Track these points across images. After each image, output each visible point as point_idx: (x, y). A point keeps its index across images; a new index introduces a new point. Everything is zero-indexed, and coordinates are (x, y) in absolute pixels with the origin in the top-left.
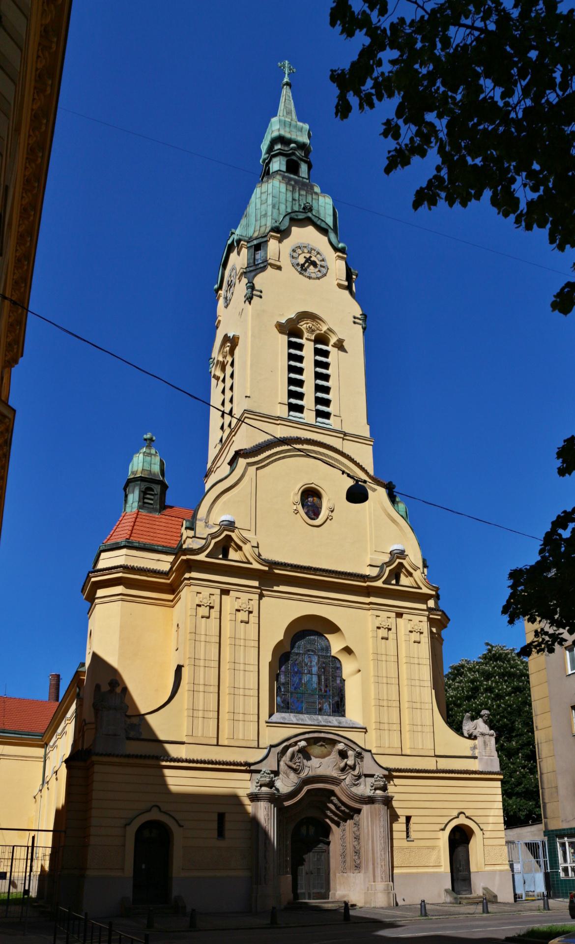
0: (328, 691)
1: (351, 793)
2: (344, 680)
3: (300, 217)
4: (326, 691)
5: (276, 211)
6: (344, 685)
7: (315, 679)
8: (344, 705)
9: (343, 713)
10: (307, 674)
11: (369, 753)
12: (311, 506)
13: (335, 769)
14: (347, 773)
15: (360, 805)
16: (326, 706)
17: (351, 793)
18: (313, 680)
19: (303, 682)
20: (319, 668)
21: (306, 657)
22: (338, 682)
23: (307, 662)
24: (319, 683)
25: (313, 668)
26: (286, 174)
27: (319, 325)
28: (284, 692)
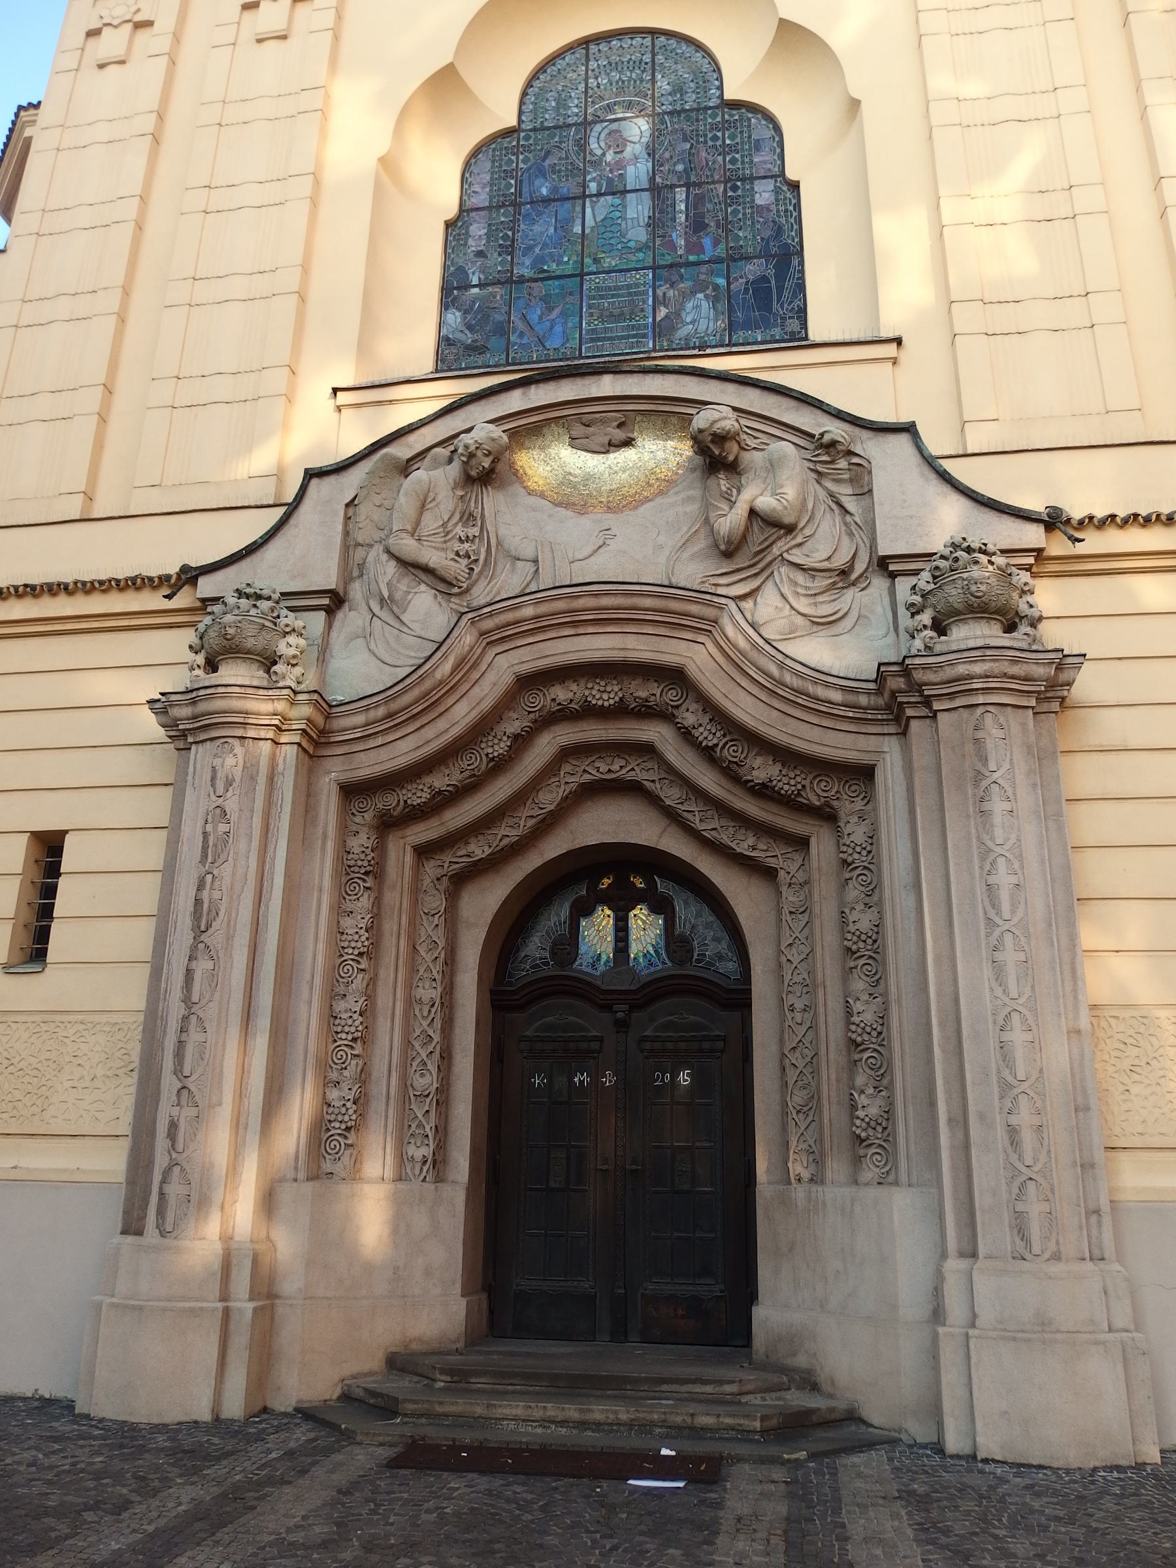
1: (782, 666)
2: (795, 186)
6: (798, 206)
7: (638, 209)
8: (801, 287)
9: (793, 325)
10: (599, 194)
11: (902, 442)
13: (693, 557)
14: (760, 566)
15: (863, 742)
16: (698, 307)
17: (782, 666)
18: (631, 213)
19: (578, 229)
21: (594, 134)
22: (764, 194)
23: (599, 152)
24: (658, 224)
25: (630, 170)
28: (480, 285)
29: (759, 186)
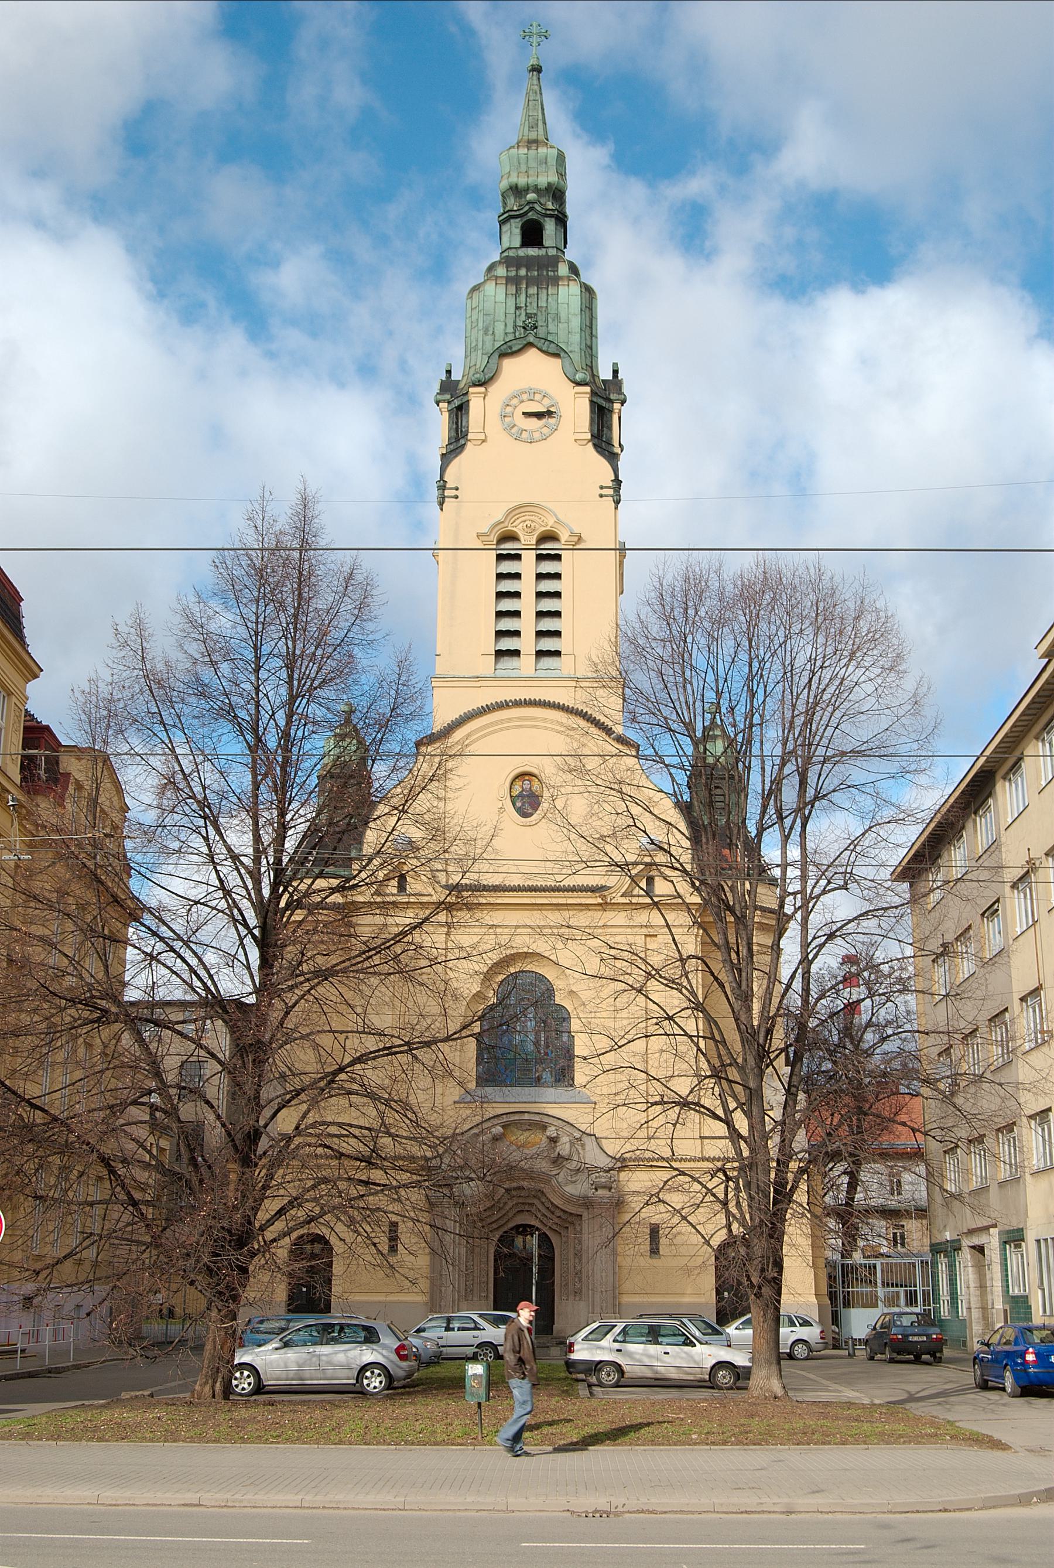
0: (549, 1052)
3: (514, 349)
4: (546, 1054)
5: (489, 338)
12: (527, 796)
20: (537, 1022)
22: (565, 1038)
26: (522, 252)
27: (543, 518)
29: (564, 1034)
